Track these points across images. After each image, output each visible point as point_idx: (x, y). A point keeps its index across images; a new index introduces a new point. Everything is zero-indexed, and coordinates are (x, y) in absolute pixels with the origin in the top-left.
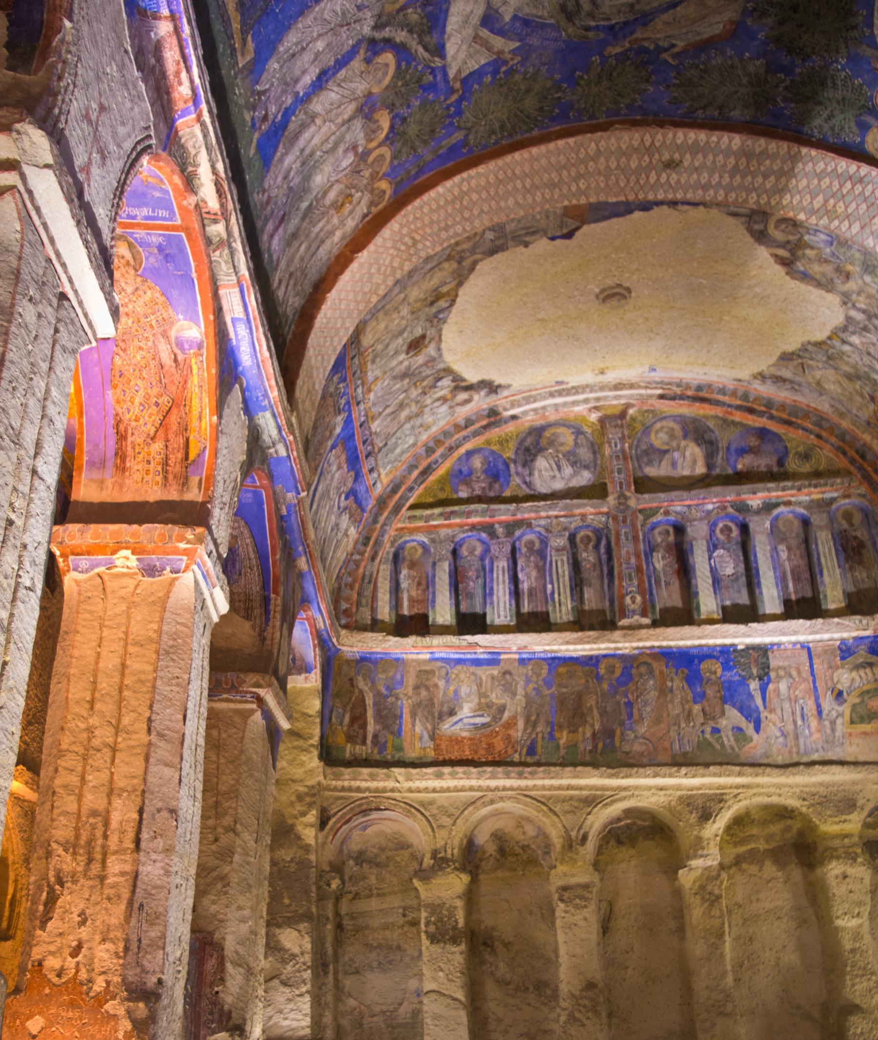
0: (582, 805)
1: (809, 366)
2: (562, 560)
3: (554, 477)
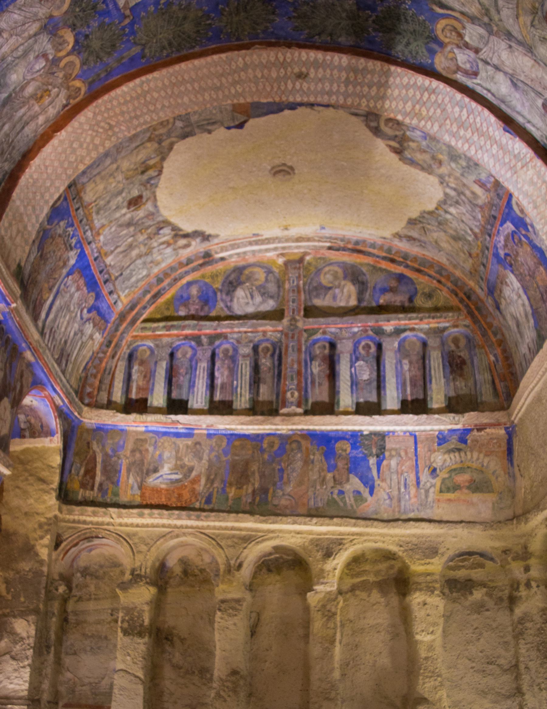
0: (240, 541)
1: (428, 229)
2: (246, 364)
3: (247, 303)
